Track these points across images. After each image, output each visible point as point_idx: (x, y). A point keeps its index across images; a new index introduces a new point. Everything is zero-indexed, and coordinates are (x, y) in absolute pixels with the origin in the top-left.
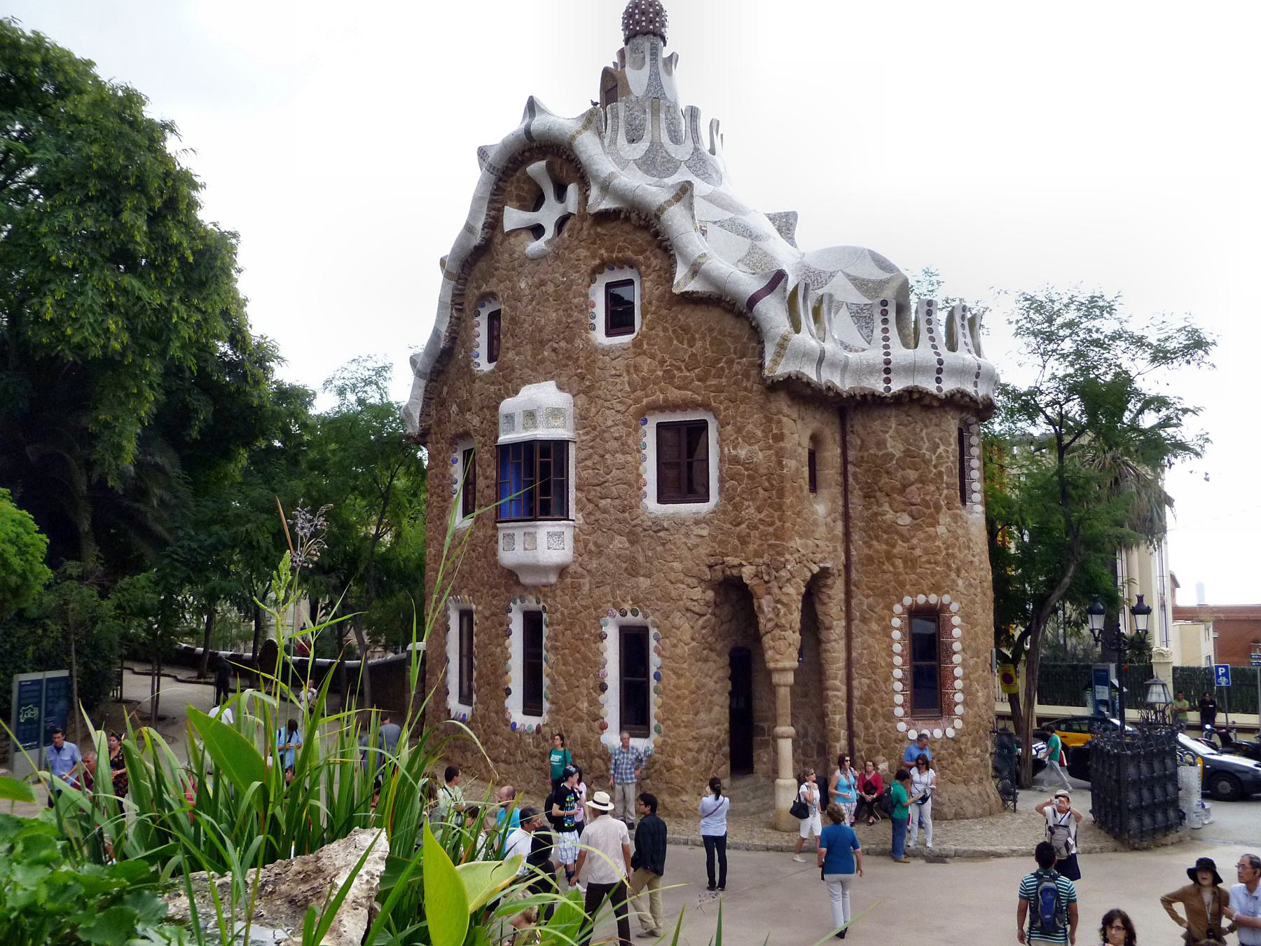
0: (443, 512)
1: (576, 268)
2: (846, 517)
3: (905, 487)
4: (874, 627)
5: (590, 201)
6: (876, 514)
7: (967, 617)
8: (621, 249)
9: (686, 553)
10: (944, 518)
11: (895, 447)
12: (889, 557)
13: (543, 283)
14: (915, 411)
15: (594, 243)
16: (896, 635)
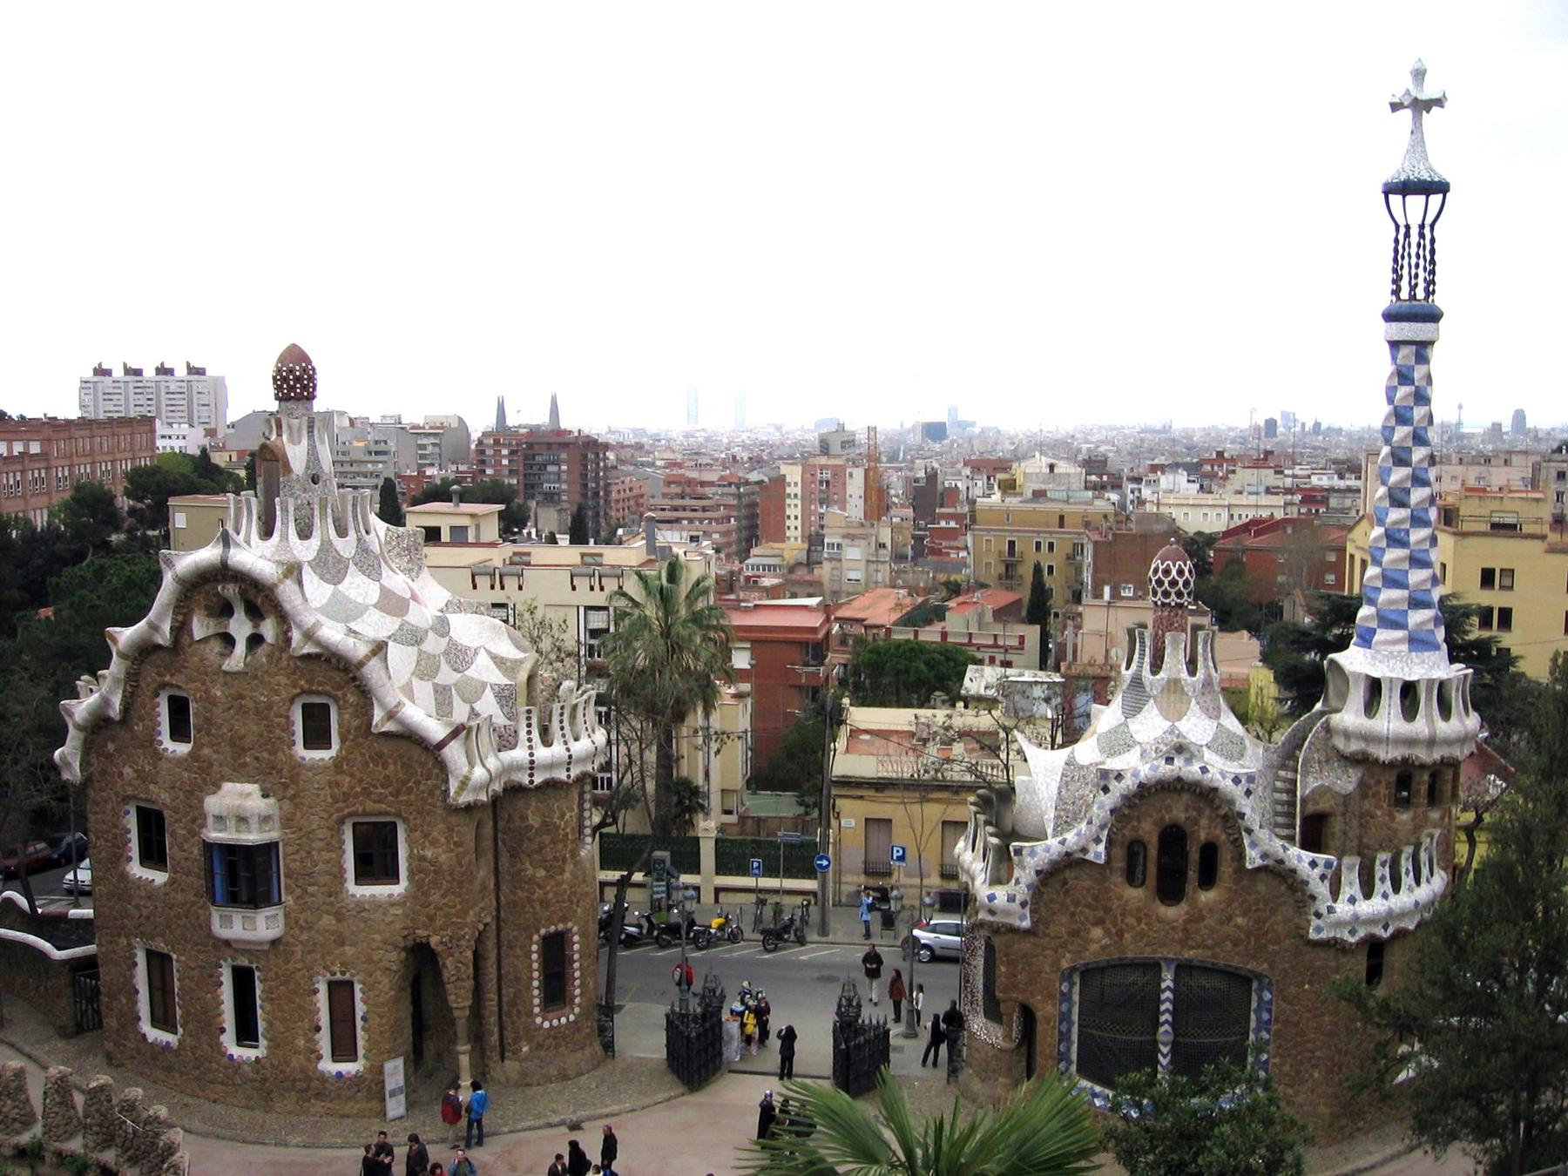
0: (119, 857)
1: (277, 693)
2: (497, 872)
3: (541, 849)
4: (519, 952)
5: (294, 644)
6: (520, 871)
7: (583, 934)
8: (319, 684)
9: (383, 927)
10: (569, 867)
11: (534, 820)
12: (530, 901)
13: (241, 697)
14: (550, 791)
15: (294, 673)
16: (535, 956)
